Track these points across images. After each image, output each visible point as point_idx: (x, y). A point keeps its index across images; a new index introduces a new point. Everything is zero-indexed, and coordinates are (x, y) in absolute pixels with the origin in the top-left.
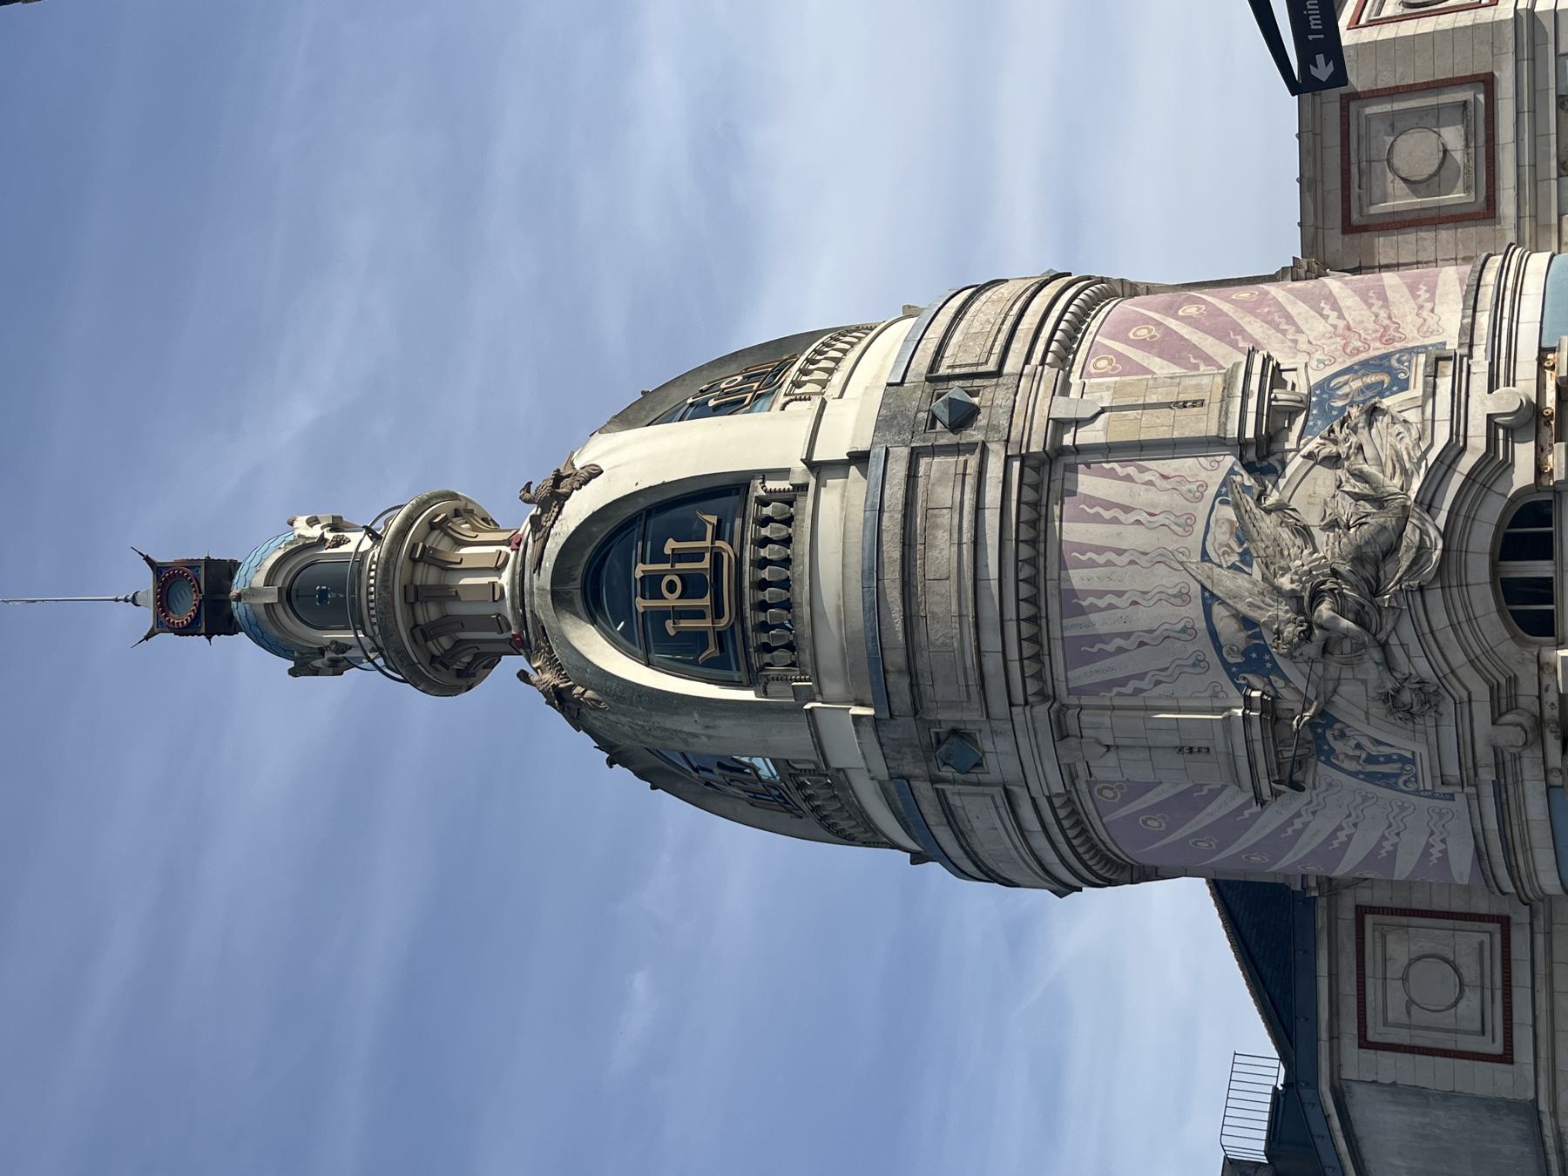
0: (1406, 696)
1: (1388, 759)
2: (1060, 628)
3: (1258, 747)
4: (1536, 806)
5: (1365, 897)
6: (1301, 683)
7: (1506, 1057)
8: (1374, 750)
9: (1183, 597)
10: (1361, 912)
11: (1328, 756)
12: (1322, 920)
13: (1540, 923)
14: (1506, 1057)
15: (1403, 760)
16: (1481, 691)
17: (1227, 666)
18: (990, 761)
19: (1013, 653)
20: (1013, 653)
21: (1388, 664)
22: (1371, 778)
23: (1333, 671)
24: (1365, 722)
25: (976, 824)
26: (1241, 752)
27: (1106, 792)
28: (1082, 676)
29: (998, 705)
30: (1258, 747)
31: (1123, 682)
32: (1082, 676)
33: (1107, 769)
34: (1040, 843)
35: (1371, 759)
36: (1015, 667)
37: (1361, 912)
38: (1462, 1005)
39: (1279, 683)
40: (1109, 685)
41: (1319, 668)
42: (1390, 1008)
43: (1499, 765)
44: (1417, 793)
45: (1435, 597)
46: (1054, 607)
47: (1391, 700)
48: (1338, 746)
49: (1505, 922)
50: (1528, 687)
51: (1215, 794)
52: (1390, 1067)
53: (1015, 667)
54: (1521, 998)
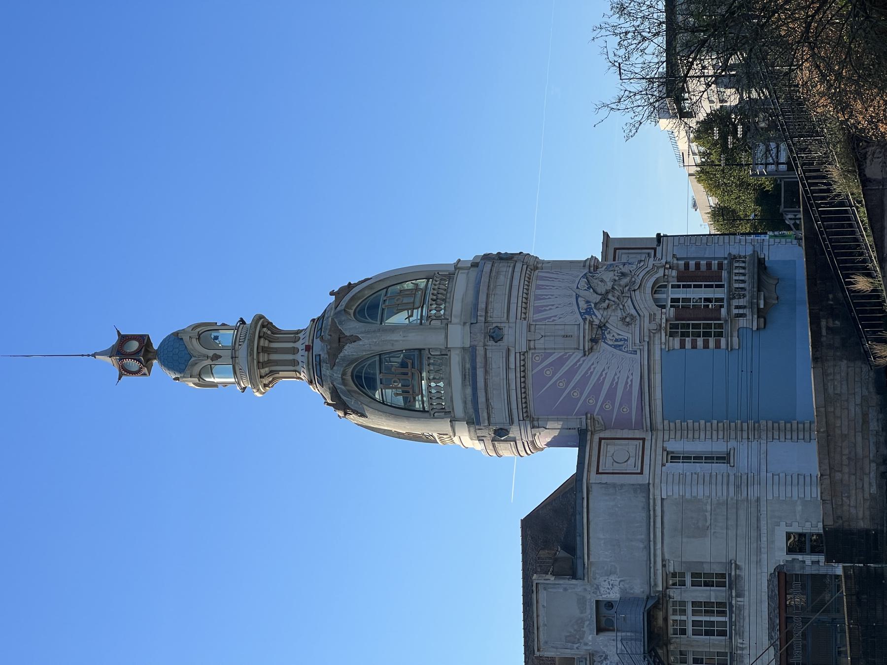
0: (628, 320)
1: (621, 340)
2: (532, 302)
3: (587, 331)
4: (657, 356)
5: (602, 435)
6: (600, 317)
7: (641, 473)
8: (617, 337)
9: (570, 296)
10: (601, 439)
11: (604, 339)
12: (589, 437)
13: (654, 437)
14: (641, 473)
15: (625, 340)
16: (647, 315)
17: (580, 313)
18: (505, 338)
19: (520, 304)
20: (520, 304)
21: (624, 309)
22: (615, 347)
23: (609, 313)
24: (616, 329)
25: (494, 366)
26: (582, 335)
27: (537, 358)
28: (538, 316)
29: (512, 319)
30: (587, 331)
31: (550, 318)
32: (538, 316)
33: (540, 344)
34: (512, 375)
35: (616, 340)
36: (519, 309)
37: (601, 439)
38: (629, 462)
39: (594, 317)
40: (545, 319)
41: (605, 313)
42: (607, 464)
43: (650, 337)
44: (627, 352)
45: (637, 292)
46: (532, 298)
47: (623, 319)
48: (608, 336)
49: (644, 440)
50: (658, 317)
51: (570, 356)
52: (605, 478)
53: (519, 309)
54: (647, 452)
